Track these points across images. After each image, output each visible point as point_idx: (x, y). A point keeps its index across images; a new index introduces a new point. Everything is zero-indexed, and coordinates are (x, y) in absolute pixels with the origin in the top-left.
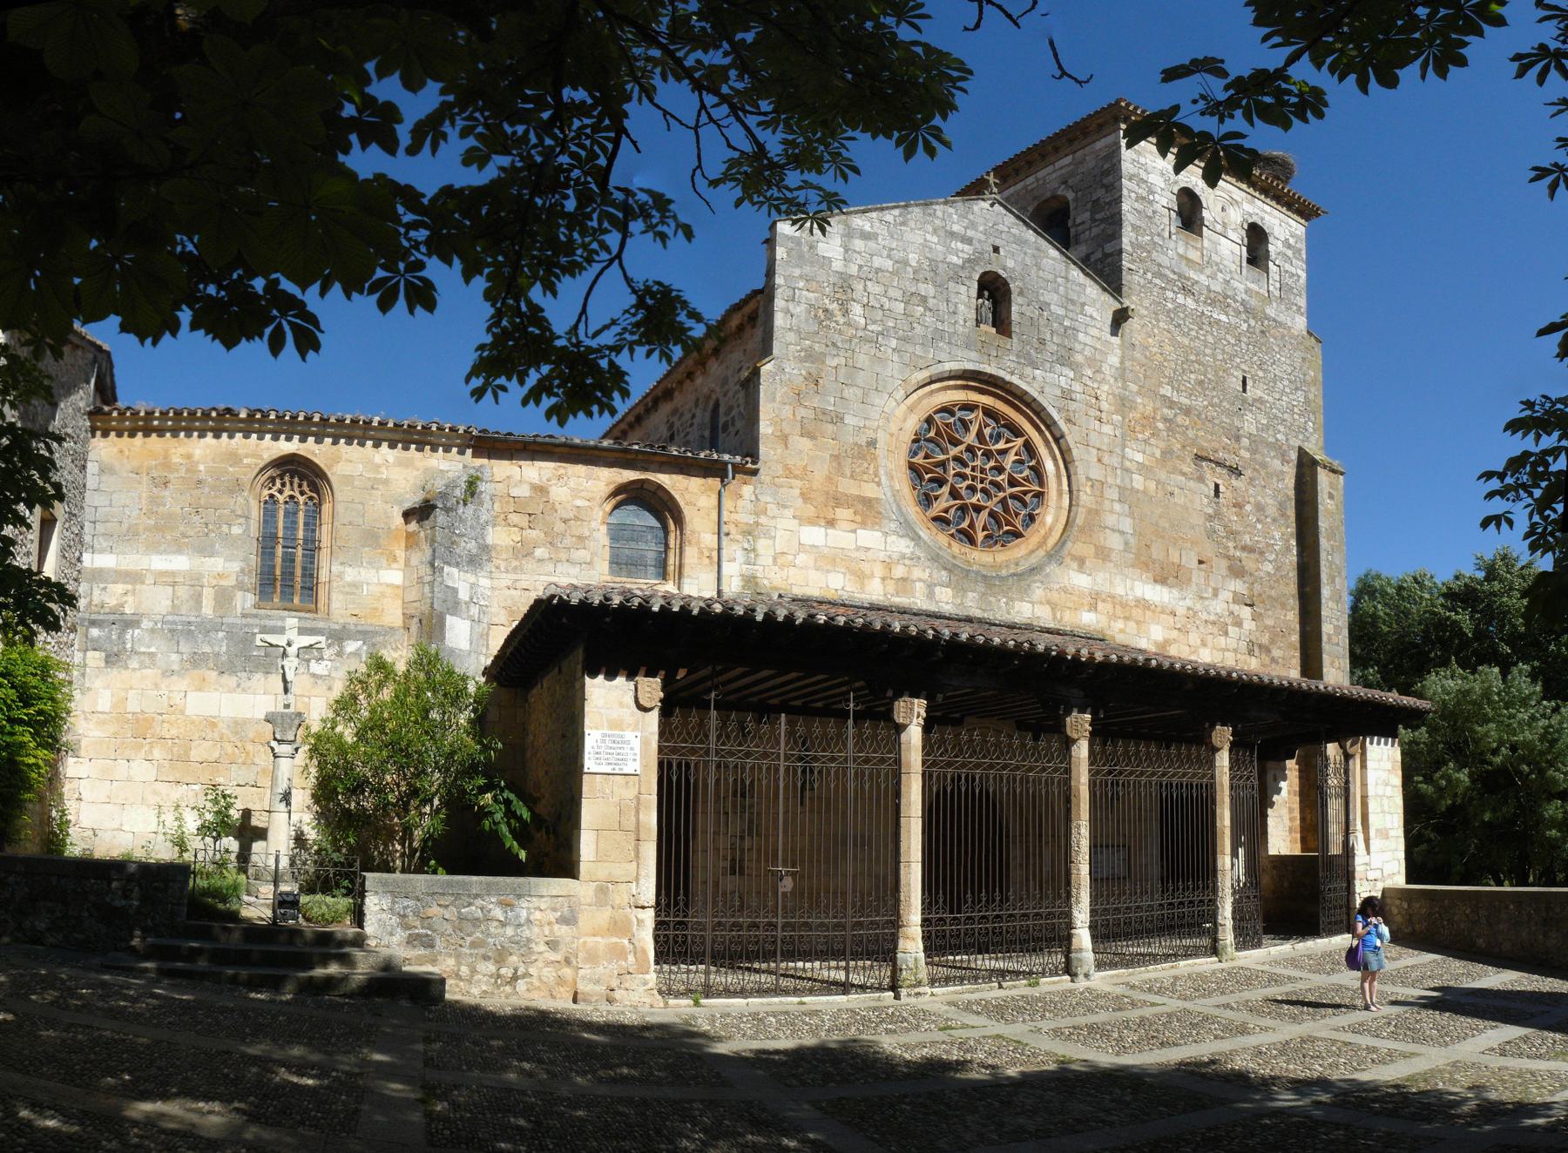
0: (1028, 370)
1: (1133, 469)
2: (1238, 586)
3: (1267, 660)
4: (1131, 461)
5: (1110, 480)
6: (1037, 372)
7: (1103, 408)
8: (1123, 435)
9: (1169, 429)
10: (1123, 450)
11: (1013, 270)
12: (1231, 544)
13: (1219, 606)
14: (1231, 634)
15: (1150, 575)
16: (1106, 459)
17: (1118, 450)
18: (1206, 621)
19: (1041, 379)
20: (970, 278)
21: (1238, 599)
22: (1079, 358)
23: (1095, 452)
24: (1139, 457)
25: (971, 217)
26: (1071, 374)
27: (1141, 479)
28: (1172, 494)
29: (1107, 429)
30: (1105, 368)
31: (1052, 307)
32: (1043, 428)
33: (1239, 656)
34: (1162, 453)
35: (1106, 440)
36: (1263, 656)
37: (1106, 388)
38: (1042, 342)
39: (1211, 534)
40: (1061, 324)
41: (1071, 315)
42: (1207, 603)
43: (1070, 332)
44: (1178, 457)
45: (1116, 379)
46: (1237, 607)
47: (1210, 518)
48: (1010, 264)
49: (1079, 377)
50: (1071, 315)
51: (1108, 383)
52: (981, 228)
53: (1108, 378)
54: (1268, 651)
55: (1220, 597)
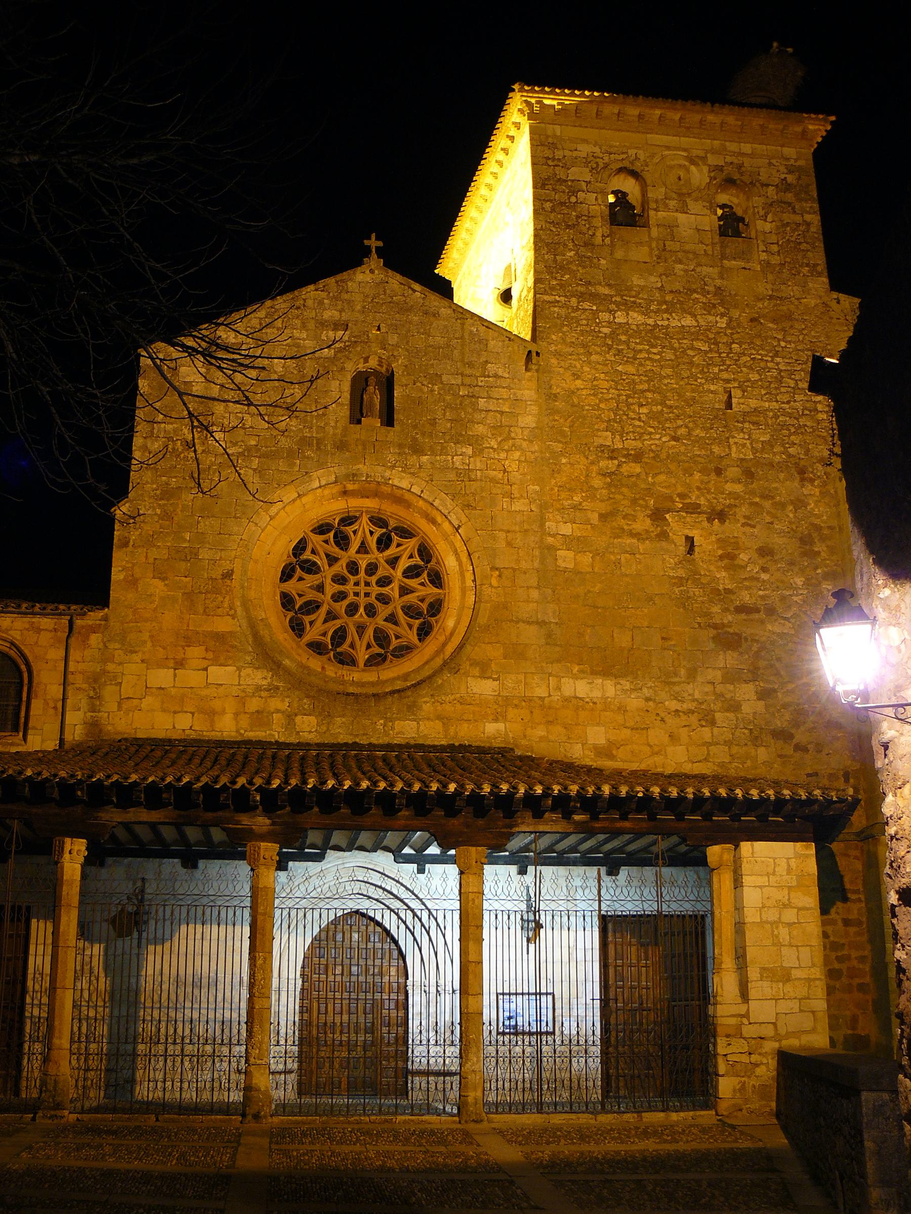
0: (413, 460)
1: (558, 545)
2: (729, 659)
3: (789, 750)
4: (554, 536)
5: (524, 565)
6: (425, 459)
7: (512, 480)
8: (543, 507)
9: (609, 485)
10: (542, 525)
11: (397, 346)
12: (716, 609)
13: (697, 690)
14: (719, 723)
15: (586, 667)
16: (519, 540)
17: (535, 527)
18: (677, 711)
19: (429, 466)
20: (343, 369)
21: (731, 677)
22: (480, 429)
23: (502, 535)
24: (566, 529)
25: (345, 296)
26: (469, 451)
27: (571, 554)
28: (618, 563)
29: (518, 506)
30: (517, 433)
31: (444, 378)
32: (439, 519)
33: (735, 749)
34: (603, 517)
35: (519, 518)
36: (780, 743)
37: (517, 454)
38: (433, 423)
39: (684, 601)
40: (456, 395)
41: (467, 381)
42: (677, 688)
43: (467, 401)
44: (625, 517)
45: (531, 441)
46: (731, 687)
47: (681, 581)
48: (393, 339)
49: (479, 452)
50: (467, 381)
51: (519, 448)
52: (359, 307)
53: (518, 442)
54: (791, 736)
55: (700, 679)
